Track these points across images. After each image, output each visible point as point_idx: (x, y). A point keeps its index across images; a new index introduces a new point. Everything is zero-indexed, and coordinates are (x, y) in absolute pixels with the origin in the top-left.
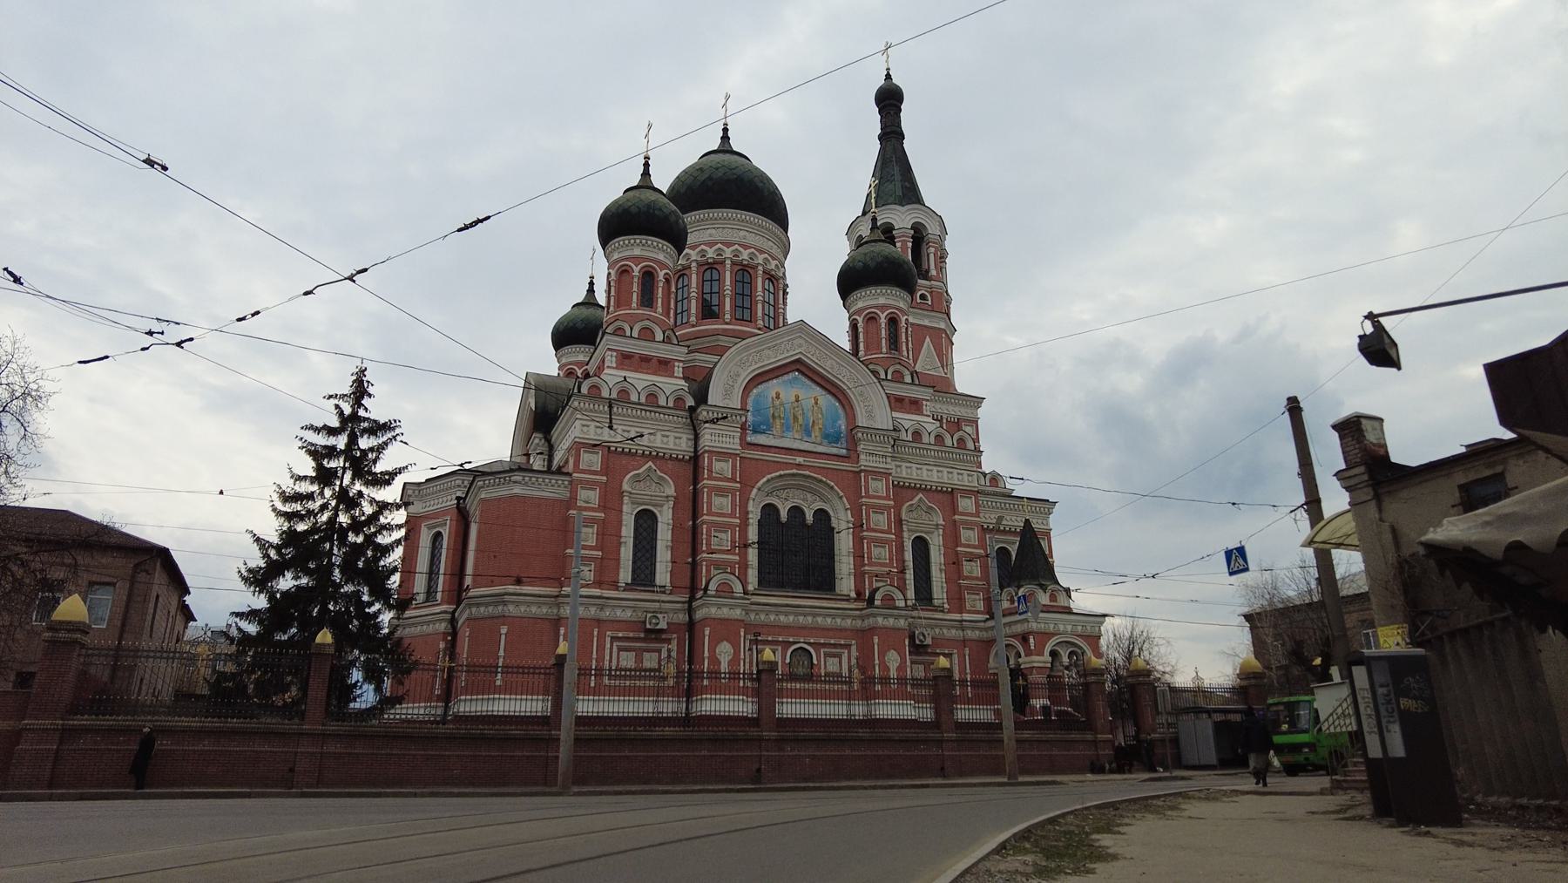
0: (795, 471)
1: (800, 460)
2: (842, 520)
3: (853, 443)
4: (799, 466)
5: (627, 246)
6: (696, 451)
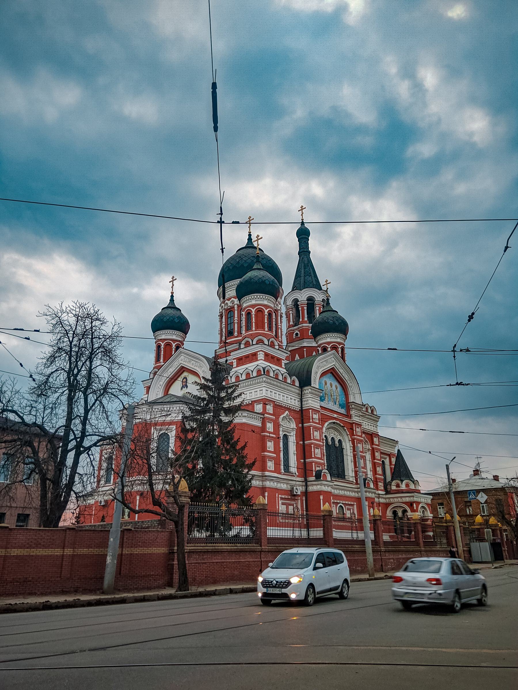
0: (334, 421)
1: (335, 416)
2: (347, 446)
3: (348, 409)
4: (335, 418)
5: (261, 298)
6: (302, 407)
